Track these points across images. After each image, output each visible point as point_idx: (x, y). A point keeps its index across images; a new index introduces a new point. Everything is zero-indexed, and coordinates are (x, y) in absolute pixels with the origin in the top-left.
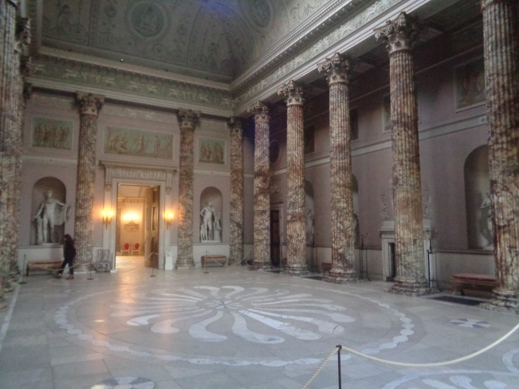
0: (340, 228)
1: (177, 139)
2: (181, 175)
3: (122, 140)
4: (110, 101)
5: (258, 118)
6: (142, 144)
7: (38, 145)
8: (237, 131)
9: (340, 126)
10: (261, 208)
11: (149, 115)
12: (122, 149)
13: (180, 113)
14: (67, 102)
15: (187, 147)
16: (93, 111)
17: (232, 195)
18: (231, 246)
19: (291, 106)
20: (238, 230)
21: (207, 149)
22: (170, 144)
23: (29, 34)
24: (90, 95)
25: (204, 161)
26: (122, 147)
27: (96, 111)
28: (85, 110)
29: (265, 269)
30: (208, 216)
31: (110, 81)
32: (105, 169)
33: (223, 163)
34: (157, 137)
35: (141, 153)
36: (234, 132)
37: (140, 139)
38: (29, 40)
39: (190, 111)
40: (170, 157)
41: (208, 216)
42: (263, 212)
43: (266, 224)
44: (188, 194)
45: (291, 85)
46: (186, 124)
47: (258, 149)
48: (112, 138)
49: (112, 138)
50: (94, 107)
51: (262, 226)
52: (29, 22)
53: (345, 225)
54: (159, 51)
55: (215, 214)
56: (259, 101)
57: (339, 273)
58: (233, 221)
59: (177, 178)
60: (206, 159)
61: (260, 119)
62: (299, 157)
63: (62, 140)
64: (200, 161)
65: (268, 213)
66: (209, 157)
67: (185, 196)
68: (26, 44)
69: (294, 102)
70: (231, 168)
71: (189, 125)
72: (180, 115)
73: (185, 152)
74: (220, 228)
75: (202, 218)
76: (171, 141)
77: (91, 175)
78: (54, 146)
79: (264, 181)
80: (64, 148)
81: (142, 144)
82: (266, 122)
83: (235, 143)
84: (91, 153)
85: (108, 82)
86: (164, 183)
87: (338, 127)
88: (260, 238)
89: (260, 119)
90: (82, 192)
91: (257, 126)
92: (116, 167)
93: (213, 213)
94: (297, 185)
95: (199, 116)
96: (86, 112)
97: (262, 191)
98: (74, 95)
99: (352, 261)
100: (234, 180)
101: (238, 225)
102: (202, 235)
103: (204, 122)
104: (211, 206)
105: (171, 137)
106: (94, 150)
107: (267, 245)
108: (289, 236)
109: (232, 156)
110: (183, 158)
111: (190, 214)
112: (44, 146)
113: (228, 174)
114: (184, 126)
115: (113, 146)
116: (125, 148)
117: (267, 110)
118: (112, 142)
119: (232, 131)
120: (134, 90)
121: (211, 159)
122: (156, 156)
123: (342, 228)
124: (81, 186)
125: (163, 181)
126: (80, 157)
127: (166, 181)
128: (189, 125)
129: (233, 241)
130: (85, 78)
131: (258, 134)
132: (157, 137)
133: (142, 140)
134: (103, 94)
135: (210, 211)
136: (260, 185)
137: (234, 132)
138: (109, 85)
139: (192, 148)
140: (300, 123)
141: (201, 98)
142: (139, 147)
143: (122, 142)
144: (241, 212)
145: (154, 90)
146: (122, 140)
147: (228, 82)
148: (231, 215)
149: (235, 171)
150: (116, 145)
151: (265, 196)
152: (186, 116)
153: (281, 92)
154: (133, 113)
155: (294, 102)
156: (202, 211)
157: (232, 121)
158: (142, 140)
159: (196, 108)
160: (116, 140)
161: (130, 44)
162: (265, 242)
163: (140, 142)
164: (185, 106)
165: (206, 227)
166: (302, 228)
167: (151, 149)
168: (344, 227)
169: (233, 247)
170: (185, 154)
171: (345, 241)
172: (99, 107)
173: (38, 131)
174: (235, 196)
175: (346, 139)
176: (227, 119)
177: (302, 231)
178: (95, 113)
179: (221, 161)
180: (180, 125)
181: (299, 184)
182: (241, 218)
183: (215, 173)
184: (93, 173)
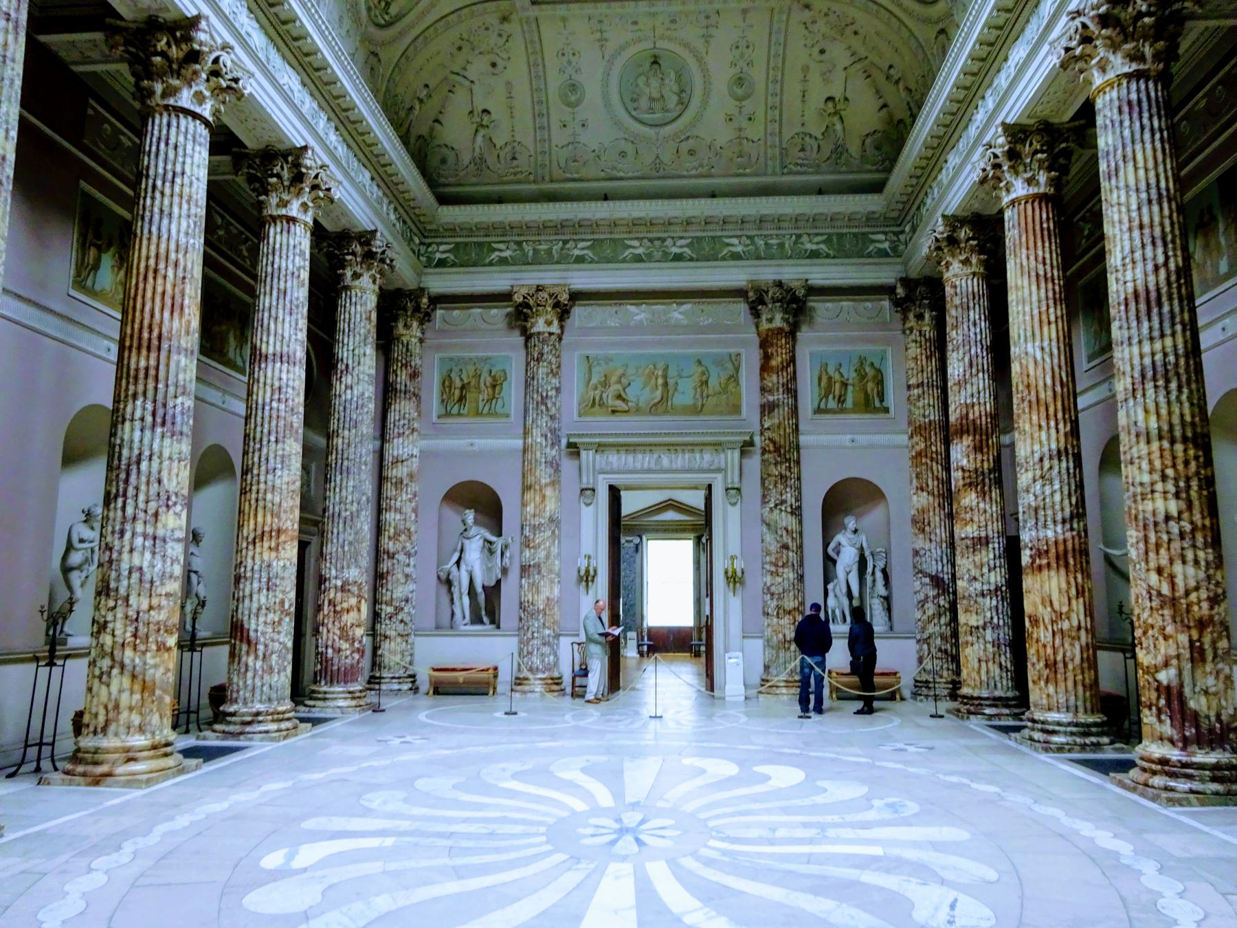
0: (1159, 594)
1: (751, 358)
2: (764, 451)
3: (619, 382)
4: (577, 296)
5: (948, 265)
6: (666, 384)
7: (448, 414)
8: (920, 317)
9: (1136, 223)
10: (971, 531)
11: (678, 313)
12: (619, 403)
13: (751, 294)
14: (498, 314)
15: (774, 378)
16: (549, 323)
17: (915, 498)
18: (918, 641)
19: (1013, 202)
20: (938, 595)
21: (837, 377)
22: (734, 378)
24: (539, 289)
25: (827, 411)
26: (619, 397)
27: (556, 323)
28: (533, 326)
29: (991, 717)
30: (847, 559)
32: (578, 454)
33: (887, 410)
34: (699, 362)
35: (660, 406)
36: (912, 322)
37: (660, 373)
39: (779, 284)
40: (736, 409)
41: (847, 559)
42: (981, 542)
43: (992, 580)
44: (783, 502)
45: (1001, 140)
46: (770, 320)
47: (955, 354)
48: (594, 381)
49: (594, 381)
50: (551, 314)
51: (978, 585)
53: (1179, 581)
54: (692, 152)
55: (867, 553)
56: (944, 216)
57: (1164, 762)
58: (921, 572)
59: (754, 463)
60: (832, 404)
61: (956, 267)
62: (1048, 359)
63: (493, 398)
64: (818, 411)
65: (997, 545)
66: (841, 400)
67: (776, 505)
69: (1020, 189)
70: (910, 423)
71: (778, 322)
72: (755, 298)
73: (770, 392)
74: (883, 592)
75: (829, 562)
76: (737, 369)
77: (550, 471)
78: (478, 414)
79: (978, 448)
80: (496, 415)
81: (666, 384)
82: (974, 274)
83: (914, 350)
84: (545, 418)
85: (577, 252)
86: (720, 476)
87: (1130, 229)
88: (974, 621)
89: (956, 267)
90: (530, 509)
91: (949, 290)
92: (600, 448)
93: (862, 549)
94: (1045, 449)
95: (801, 293)
96: (534, 330)
97: (975, 481)
98: (503, 297)
99: (1218, 716)
100: (919, 454)
101: (937, 581)
102: (833, 612)
103: (822, 308)
104: (855, 531)
105: (735, 361)
106: (553, 411)
107: (996, 644)
108: (1030, 617)
109: (909, 387)
110: (767, 409)
111: (790, 554)
112: (459, 414)
113: (903, 439)
114: (765, 326)
115: (597, 398)
116: (624, 400)
117: (973, 238)
118: (596, 389)
119: (905, 319)
120: (638, 259)
121: (849, 403)
122: (696, 410)
123: (1166, 590)
124: (528, 496)
125: (719, 470)
126: (526, 433)
127: (725, 470)
128: (778, 322)
129: (923, 629)
130: (531, 253)
131: (953, 312)
132: (699, 362)
133: (665, 377)
134: (569, 281)
135: (853, 545)
136: (965, 462)
137: (912, 322)
138: (580, 260)
139: (794, 378)
140: (1047, 252)
141: (809, 246)
142: (658, 393)
143: (619, 387)
144: (944, 545)
145: (686, 249)
146: (619, 382)
147: (877, 187)
148: (916, 553)
149: (919, 430)
150: (604, 396)
151: (983, 494)
153: (984, 170)
154: (639, 313)
155: (1020, 189)
156: (832, 545)
157: (900, 291)
158: (665, 377)
159: (793, 273)
160: (605, 383)
161: (623, 154)
162: (989, 635)
163: (660, 381)
164: (767, 273)
165: (844, 590)
166: (1073, 592)
167: (685, 394)
168: (1173, 585)
169: (925, 647)
170: (771, 398)
171: (1183, 639)
172: (563, 313)
173: (446, 383)
174: (923, 500)
175: (1166, 264)
176: (888, 290)
177: (1074, 602)
178: (555, 328)
179: (877, 404)
180: (757, 326)
181: (1054, 446)
182: (945, 561)
183: (862, 439)
184: (556, 466)
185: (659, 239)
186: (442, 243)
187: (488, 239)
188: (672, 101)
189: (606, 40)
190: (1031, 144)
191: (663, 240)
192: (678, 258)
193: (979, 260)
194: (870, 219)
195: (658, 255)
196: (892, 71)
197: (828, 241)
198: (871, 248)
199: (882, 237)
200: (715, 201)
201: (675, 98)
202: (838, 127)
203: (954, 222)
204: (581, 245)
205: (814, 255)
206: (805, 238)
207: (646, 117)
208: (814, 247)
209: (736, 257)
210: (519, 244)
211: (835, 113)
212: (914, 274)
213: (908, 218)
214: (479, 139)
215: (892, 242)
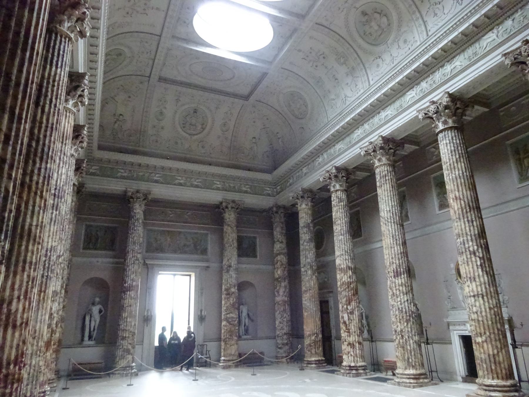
23: (86, 139)
31: (158, 177)
38: (85, 144)
39: (233, 201)
52: (86, 129)
61: (304, 206)
68: (82, 148)
89: (304, 206)
152: (229, 206)
185: (190, 178)
186: (94, 166)
187: (116, 167)
188: (199, 127)
189: (180, 100)
190: (342, 174)
191: (192, 178)
192: (197, 186)
193: (311, 205)
194: (265, 182)
195: (188, 184)
196: (278, 134)
197: (250, 188)
198: (265, 193)
199: (269, 189)
200: (211, 166)
201: (200, 126)
202: (255, 148)
203: (304, 191)
204: (157, 175)
205: (246, 192)
206: (242, 186)
207: (189, 132)
208: (246, 189)
209: (218, 189)
210: (130, 171)
211: (255, 143)
212: (280, 204)
213: (280, 184)
214: (116, 125)
215: (272, 191)
